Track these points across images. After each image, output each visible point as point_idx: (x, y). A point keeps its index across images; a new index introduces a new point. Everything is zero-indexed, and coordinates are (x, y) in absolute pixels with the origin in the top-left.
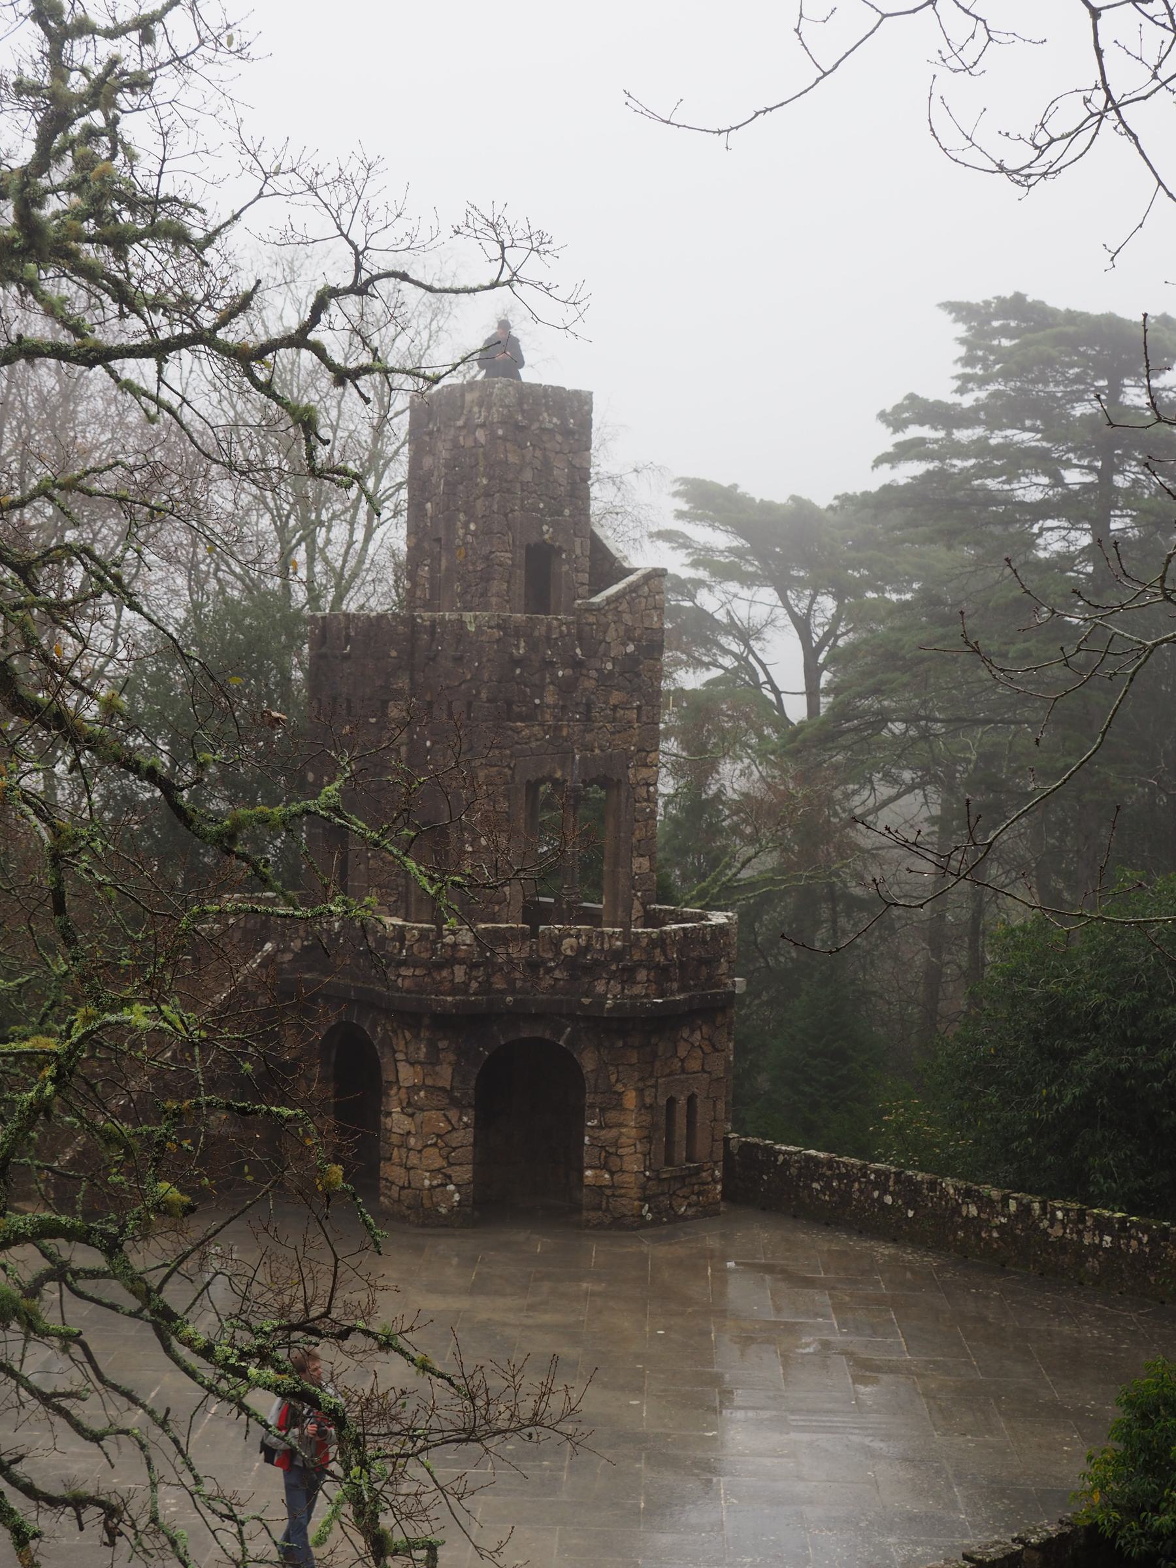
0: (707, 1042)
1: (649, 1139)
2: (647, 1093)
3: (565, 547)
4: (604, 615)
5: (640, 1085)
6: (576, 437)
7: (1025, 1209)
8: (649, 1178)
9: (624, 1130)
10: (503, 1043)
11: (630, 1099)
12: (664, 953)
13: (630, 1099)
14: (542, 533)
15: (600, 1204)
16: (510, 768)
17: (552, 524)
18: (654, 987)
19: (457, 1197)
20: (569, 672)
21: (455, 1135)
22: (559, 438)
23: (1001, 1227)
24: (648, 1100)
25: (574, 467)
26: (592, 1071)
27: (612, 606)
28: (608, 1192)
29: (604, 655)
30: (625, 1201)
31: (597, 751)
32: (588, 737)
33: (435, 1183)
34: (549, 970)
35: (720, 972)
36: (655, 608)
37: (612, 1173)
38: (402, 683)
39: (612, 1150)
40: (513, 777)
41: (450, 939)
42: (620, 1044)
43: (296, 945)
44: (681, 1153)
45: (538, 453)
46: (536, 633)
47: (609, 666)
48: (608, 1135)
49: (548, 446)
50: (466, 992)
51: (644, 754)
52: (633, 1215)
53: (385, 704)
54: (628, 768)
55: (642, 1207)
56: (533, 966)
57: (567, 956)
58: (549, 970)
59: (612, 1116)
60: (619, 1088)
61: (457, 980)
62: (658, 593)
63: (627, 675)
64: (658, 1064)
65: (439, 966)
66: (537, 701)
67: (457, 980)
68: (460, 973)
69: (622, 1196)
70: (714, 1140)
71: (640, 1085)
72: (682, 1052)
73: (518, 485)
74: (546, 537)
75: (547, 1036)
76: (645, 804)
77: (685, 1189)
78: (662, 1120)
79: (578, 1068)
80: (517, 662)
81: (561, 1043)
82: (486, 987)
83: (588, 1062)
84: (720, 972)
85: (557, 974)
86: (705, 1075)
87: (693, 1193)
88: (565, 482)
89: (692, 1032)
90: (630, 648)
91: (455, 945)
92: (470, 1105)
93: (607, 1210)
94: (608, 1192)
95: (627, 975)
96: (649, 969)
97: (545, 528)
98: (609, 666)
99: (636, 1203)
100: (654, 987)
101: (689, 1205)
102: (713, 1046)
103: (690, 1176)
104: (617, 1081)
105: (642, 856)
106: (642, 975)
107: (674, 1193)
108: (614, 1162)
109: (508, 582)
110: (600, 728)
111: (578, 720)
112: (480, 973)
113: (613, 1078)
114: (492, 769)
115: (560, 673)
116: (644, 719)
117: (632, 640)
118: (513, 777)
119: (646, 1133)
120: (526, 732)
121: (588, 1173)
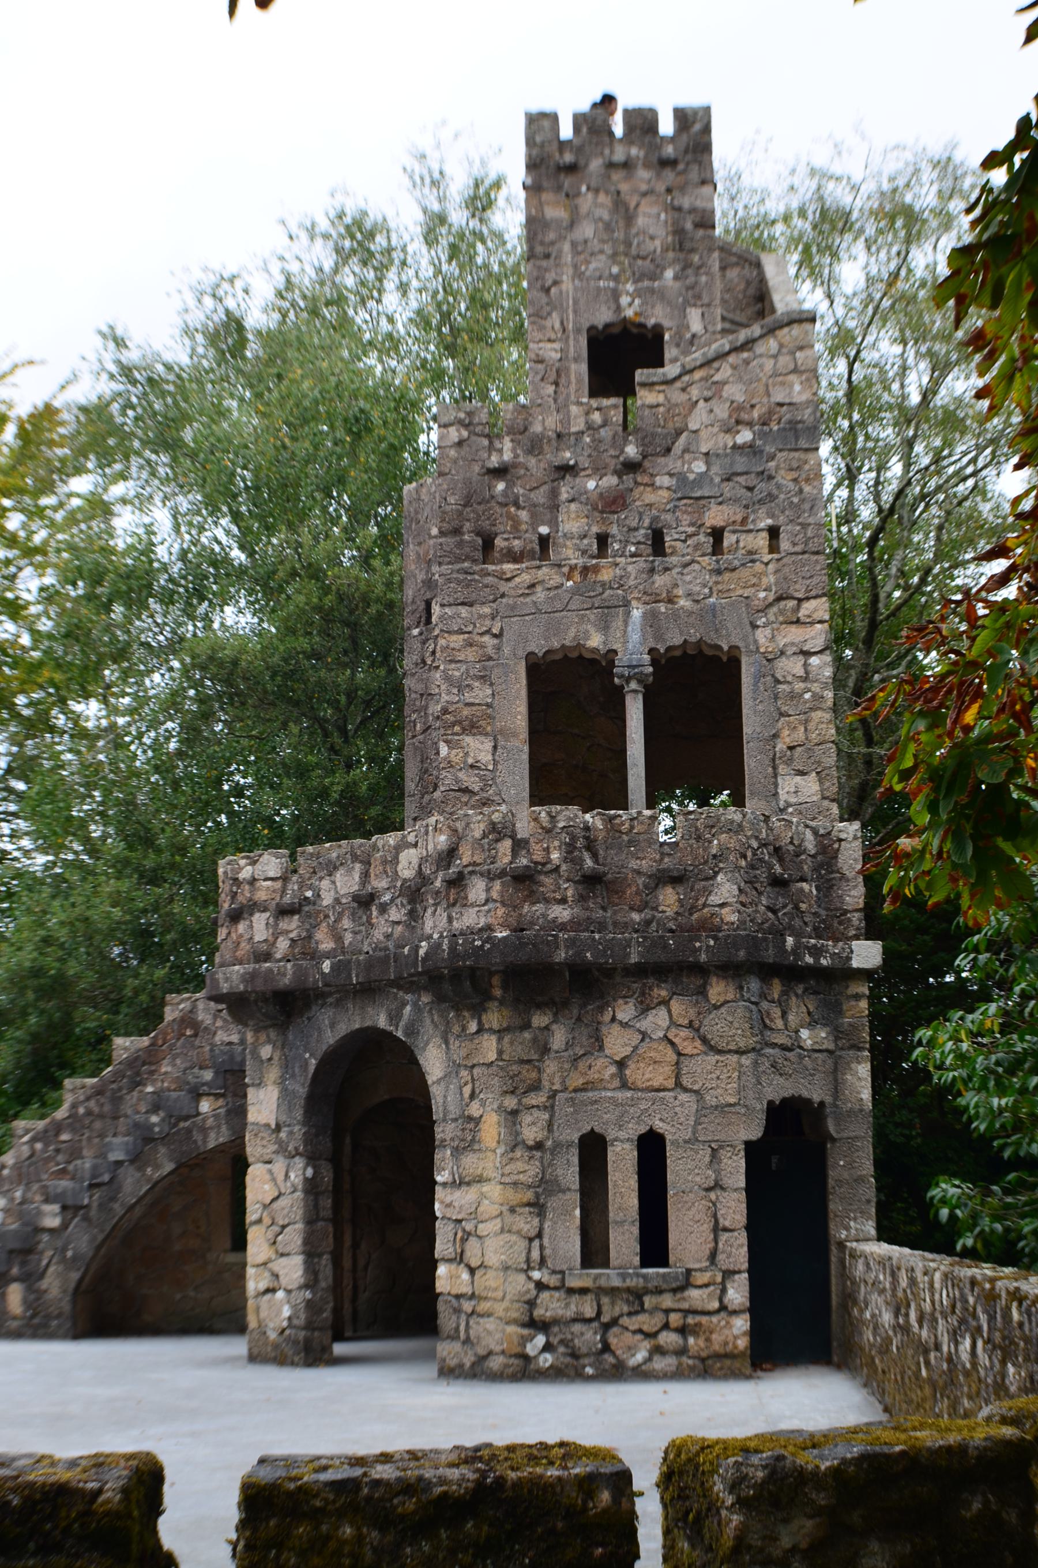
0: (684, 1033)
1: (538, 1207)
2: (527, 1119)
3: (666, 323)
4: (684, 390)
5: (511, 1102)
6: (681, 167)
8: (540, 1286)
9: (486, 1188)
10: (332, 1041)
11: (491, 1129)
13: (491, 1129)
14: (618, 308)
15: (457, 1329)
16: (495, 636)
17: (638, 293)
18: (501, 912)
19: (286, 1312)
21: (282, 1202)
22: (643, 174)
24: (531, 1133)
25: (679, 209)
26: (438, 1082)
27: (698, 375)
28: (467, 1306)
29: (686, 450)
30: (490, 1324)
31: (682, 602)
32: (660, 581)
33: (262, 1286)
34: (383, 909)
35: (714, 899)
36: (795, 371)
37: (472, 1271)
39: (469, 1226)
40: (498, 648)
42: (473, 1027)
45: (602, 198)
46: (537, 428)
47: (699, 467)
49: (624, 187)
50: (267, 956)
51: (791, 604)
52: (503, 1352)
54: (755, 627)
55: (524, 1340)
56: (365, 901)
57: (405, 880)
59: (471, 1163)
60: (475, 1109)
61: (257, 939)
62: (801, 348)
63: (741, 479)
64: (551, 1067)
66: (544, 530)
67: (257, 939)
68: (259, 926)
69: (489, 1315)
70: (717, 1229)
71: (511, 1102)
72: (618, 1043)
73: (567, 247)
74: (629, 313)
75: (382, 1022)
76: (799, 686)
77: (642, 1318)
78: (569, 1173)
80: (501, 472)
81: (400, 1034)
82: (305, 950)
83: (433, 1062)
84: (714, 899)
86: (684, 1097)
87: (666, 1326)
88: (661, 232)
89: (645, 1009)
90: (745, 436)
91: (253, 881)
92: (298, 1154)
93: (467, 1341)
94: (467, 1306)
96: (490, 877)
97: (624, 300)
98: (699, 467)
99: (512, 1329)
100: (501, 912)
101: (658, 1350)
102: (704, 1040)
103: (659, 1291)
104: (472, 1096)
105: (802, 773)
106: (477, 890)
107: (614, 1322)
108: (473, 1252)
109: (556, 384)
110: (686, 565)
111: (633, 555)
112: (292, 925)
113: (467, 1090)
114: (454, 638)
115: (591, 485)
116: (785, 545)
117: (750, 424)
118: (498, 648)
119: (529, 1195)
120: (526, 578)
121: (442, 1270)
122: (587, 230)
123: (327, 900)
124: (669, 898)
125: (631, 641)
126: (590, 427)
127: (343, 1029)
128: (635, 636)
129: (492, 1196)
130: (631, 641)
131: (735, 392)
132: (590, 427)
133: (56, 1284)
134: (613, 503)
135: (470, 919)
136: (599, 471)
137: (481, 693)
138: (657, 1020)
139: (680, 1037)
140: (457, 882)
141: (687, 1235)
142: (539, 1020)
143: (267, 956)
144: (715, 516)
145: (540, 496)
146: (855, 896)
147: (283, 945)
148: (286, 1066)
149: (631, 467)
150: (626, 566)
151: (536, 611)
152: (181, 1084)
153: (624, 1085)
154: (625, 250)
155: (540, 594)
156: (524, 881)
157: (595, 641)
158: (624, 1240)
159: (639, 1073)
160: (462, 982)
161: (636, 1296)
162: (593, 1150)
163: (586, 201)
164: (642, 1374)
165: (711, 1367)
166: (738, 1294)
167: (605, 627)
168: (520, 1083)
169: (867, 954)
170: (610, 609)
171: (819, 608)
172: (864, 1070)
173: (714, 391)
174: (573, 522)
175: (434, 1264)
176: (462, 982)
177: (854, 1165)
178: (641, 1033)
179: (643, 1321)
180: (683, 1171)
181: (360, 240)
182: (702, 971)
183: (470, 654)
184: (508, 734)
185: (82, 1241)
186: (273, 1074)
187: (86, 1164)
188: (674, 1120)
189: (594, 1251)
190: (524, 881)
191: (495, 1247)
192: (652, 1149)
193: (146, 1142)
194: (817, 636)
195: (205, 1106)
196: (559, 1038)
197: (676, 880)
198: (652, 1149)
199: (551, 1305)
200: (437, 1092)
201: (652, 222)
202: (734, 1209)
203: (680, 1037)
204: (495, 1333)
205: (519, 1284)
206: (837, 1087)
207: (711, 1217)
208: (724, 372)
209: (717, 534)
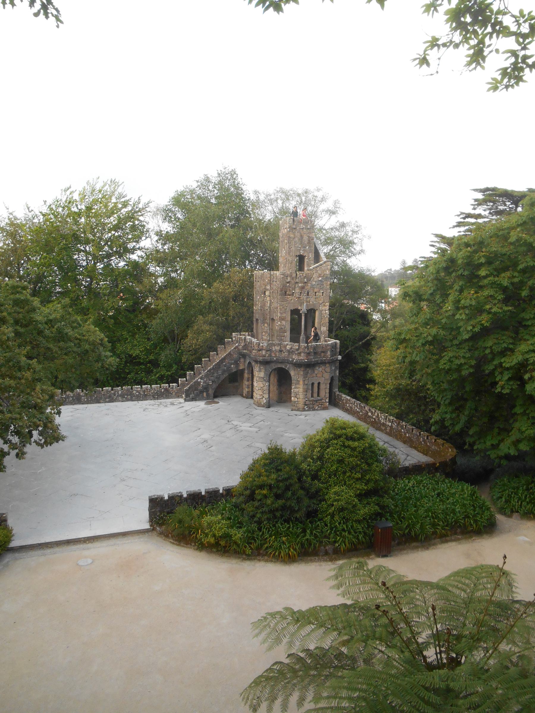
1: (306, 391)
7: (378, 415)
12: (308, 349)
13: (301, 383)
17: (303, 250)
20: (302, 284)
23: (374, 419)
24: (306, 383)
32: (308, 299)
34: (284, 352)
38: (268, 287)
41: (261, 345)
43: (242, 344)
44: (315, 395)
48: (296, 390)
50: (265, 356)
53: (265, 292)
58: (284, 352)
59: (298, 386)
60: (299, 379)
64: (309, 375)
65: (259, 350)
68: (264, 352)
70: (326, 393)
72: (316, 372)
75: (283, 367)
78: (310, 387)
79: (290, 375)
82: (270, 355)
83: (292, 373)
85: (286, 353)
89: (319, 367)
90: (320, 279)
95: (299, 354)
96: (304, 353)
106: (302, 354)
108: (298, 396)
116: (324, 295)
122: (297, 239)
123: (274, 349)
124: (323, 354)
125: (303, 309)
126: (300, 276)
127: (276, 367)
128: (305, 307)
129: (301, 390)
130: (303, 309)
131: (319, 272)
132: (300, 276)
133: (211, 392)
134: (303, 288)
135: (301, 358)
136: (301, 283)
137: (284, 315)
138: (321, 369)
139: (323, 371)
140: (300, 353)
141: (322, 393)
142: (308, 369)
143: (265, 356)
144: (316, 290)
145: (293, 286)
146: (338, 350)
147: (267, 355)
148: (266, 370)
149: (305, 282)
150: (304, 297)
151: (292, 302)
152: (229, 363)
153: (317, 376)
154: (301, 243)
155: (293, 301)
156: (309, 354)
157: (300, 308)
158: (315, 395)
159: (318, 375)
160: (298, 365)
161: (317, 401)
162: (313, 384)
163: (296, 234)
164: (317, 410)
165: (325, 408)
166: (327, 400)
167: (301, 306)
168: (305, 376)
169: (340, 358)
170: (301, 304)
171: (328, 304)
172: (338, 371)
173: (317, 272)
174: (297, 290)
175: (291, 397)
176: (298, 365)
177: (336, 383)
178: (319, 370)
179: (317, 404)
180: (322, 386)
181: (207, 179)
182: (326, 363)
183: (283, 309)
184: (287, 321)
185: (215, 386)
186: (263, 370)
187: (215, 375)
188: (322, 380)
189: (312, 396)
190: (309, 354)
191: (301, 396)
192: (319, 384)
193: (224, 371)
194: (327, 308)
195: (232, 366)
196: (310, 372)
197: (323, 352)
198: (319, 384)
199: (308, 403)
200: (293, 377)
201: (305, 238)
202: (328, 391)
203: (323, 371)
204: (301, 405)
205: (304, 400)
206: (335, 374)
207: (325, 392)
208: (318, 269)
209: (316, 293)
